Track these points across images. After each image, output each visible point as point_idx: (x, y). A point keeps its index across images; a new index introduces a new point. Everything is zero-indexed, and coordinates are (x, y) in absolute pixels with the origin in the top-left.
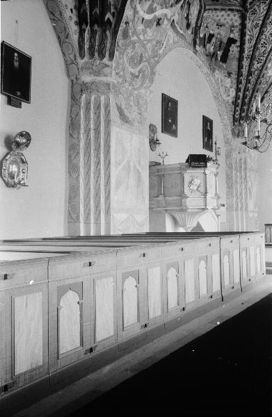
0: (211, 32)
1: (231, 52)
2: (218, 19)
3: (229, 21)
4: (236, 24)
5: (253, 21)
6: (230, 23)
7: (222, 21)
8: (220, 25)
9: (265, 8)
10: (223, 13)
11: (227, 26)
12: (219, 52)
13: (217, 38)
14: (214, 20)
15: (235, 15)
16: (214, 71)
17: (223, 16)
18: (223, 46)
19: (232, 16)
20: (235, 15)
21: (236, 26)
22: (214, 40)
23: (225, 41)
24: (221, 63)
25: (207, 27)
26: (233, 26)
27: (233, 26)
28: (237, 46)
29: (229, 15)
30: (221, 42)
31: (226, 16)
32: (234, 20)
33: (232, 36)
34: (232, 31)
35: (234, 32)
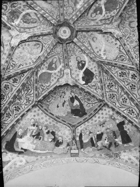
0: (98, 133)
1: (128, 131)
2: (97, 122)
3: (106, 116)
4: (111, 113)
5: (118, 100)
6: (107, 116)
7: (102, 120)
8: (102, 124)
9: (116, 87)
10: (97, 115)
11: (108, 120)
12: (116, 140)
13: (107, 133)
14: (94, 125)
15: (105, 110)
16: (117, 155)
17: (99, 117)
18: (118, 133)
19: (104, 112)
20: (105, 110)
21: (113, 114)
22: (104, 136)
23: (116, 129)
24: (125, 145)
25: (90, 133)
26: (111, 117)
27: (111, 117)
28: (128, 124)
29: (102, 114)
30: (114, 133)
31: (101, 116)
32: (108, 113)
33: (118, 122)
34: (114, 119)
35: (116, 118)
